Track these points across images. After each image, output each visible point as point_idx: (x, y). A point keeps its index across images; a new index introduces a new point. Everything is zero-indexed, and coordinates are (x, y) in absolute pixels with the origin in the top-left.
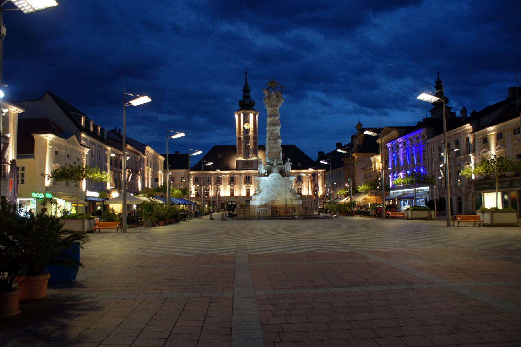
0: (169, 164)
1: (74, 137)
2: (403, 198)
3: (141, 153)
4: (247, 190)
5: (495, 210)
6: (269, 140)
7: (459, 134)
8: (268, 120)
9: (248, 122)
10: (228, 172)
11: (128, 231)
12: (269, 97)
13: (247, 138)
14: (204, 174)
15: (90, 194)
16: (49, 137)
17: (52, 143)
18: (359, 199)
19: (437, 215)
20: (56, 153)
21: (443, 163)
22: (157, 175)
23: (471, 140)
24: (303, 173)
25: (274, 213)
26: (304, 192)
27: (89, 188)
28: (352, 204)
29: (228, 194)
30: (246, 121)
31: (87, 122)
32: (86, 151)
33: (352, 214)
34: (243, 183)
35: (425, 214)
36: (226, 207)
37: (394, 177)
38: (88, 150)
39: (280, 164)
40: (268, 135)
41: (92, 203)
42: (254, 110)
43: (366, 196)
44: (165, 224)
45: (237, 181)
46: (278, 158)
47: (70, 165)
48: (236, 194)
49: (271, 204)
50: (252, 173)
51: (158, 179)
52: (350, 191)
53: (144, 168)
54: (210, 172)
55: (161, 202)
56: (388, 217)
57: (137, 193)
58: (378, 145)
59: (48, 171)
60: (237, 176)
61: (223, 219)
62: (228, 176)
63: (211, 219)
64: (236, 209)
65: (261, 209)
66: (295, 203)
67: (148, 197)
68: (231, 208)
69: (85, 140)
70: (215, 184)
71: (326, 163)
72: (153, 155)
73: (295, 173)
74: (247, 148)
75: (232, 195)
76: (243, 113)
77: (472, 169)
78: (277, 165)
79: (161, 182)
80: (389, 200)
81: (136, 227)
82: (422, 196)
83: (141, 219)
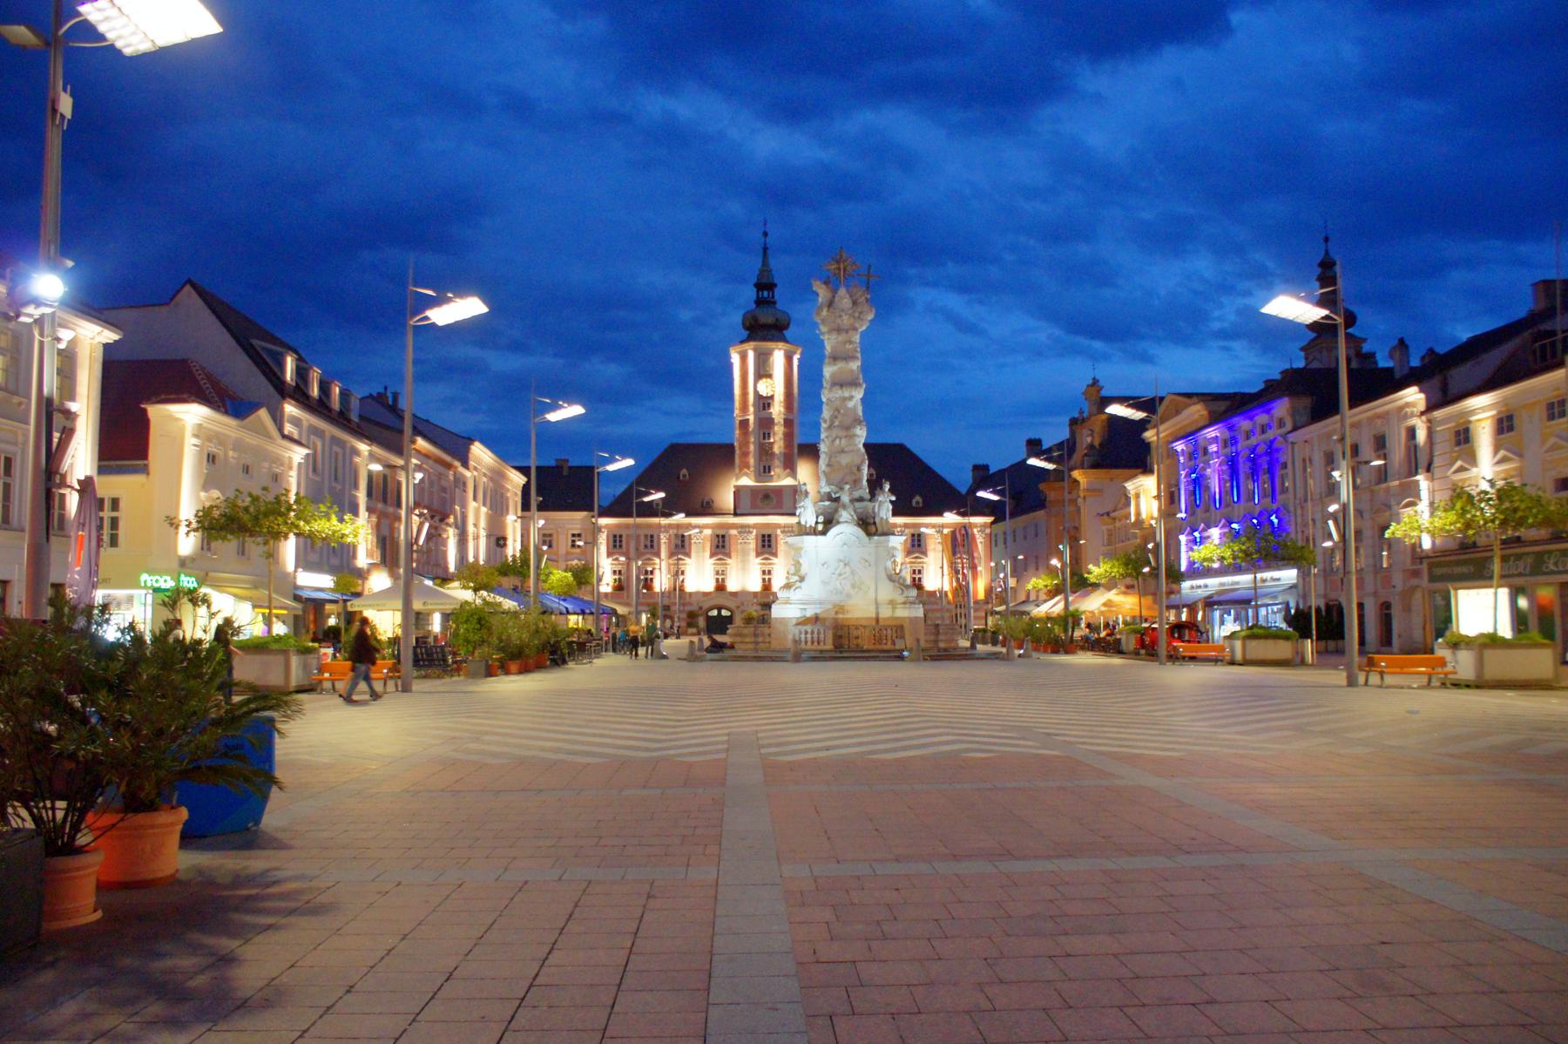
0: (538, 494)
1: (263, 413)
2: (1219, 603)
3: (457, 464)
5: (1491, 641)
6: (830, 427)
7: (1384, 416)
8: (828, 371)
9: (770, 376)
11: (414, 688)
12: (830, 304)
13: (766, 423)
14: (638, 526)
17: (199, 432)
20: (212, 458)
21: (1337, 499)
22: (503, 526)
23: (1421, 435)
24: (927, 526)
25: (842, 641)
27: (304, 562)
28: (1070, 619)
29: (709, 586)
30: (763, 372)
31: (301, 373)
32: (298, 454)
33: (1068, 647)
34: (753, 554)
35: (1283, 649)
36: (702, 622)
37: (1195, 541)
38: (304, 451)
39: (861, 499)
40: (826, 413)
42: (786, 341)
43: (1112, 595)
44: (525, 670)
45: (736, 546)
46: (856, 483)
47: (250, 495)
48: (732, 586)
49: (832, 615)
50: (778, 526)
51: (505, 539)
52: (1064, 580)
53: (464, 506)
54: (656, 520)
55: (509, 604)
56: (1174, 657)
57: (445, 579)
58: (1146, 446)
59: (187, 511)
60: (734, 532)
61: (692, 657)
62: (708, 532)
64: (726, 628)
65: (804, 628)
66: (902, 613)
67: (476, 590)
68: (718, 625)
69: (296, 422)
70: (671, 555)
71: (996, 498)
72: (492, 470)
73: (906, 526)
74: (765, 452)
75: (721, 587)
76: (755, 350)
77: (1422, 521)
78: (853, 501)
79: (513, 548)
80: (1178, 608)
81: (439, 677)
82: (1275, 597)
83: (455, 654)
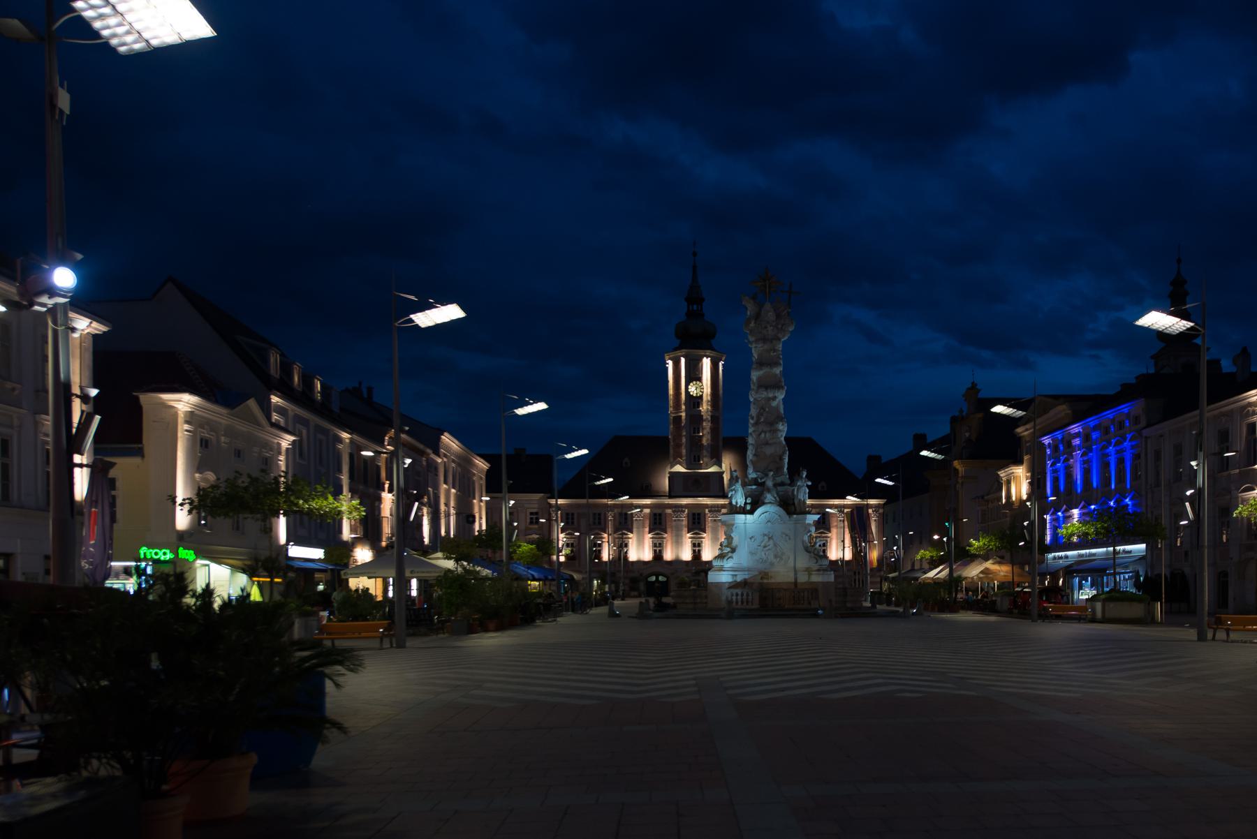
0: (509, 478)
1: (252, 403)
2: (1078, 571)
3: (429, 451)
4: (694, 545)
6: (756, 424)
7: (1229, 414)
8: (755, 375)
10: (648, 501)
11: (408, 644)
13: (695, 418)
14: (588, 505)
15: (296, 551)
16: (184, 402)
17: (191, 418)
18: (973, 571)
19: (1167, 612)
20: (205, 443)
21: (1192, 484)
22: (471, 506)
24: (831, 507)
26: (834, 553)
28: (953, 582)
29: (647, 555)
30: (694, 375)
32: (286, 441)
33: (953, 607)
34: (685, 529)
35: (1137, 610)
36: (642, 586)
37: (1057, 519)
38: (292, 438)
39: (782, 484)
40: (753, 411)
41: (305, 571)
42: (713, 349)
43: (989, 565)
44: (500, 628)
46: (778, 470)
47: (249, 476)
48: (668, 555)
49: (759, 580)
50: (706, 506)
51: (474, 517)
52: (949, 552)
53: (436, 488)
54: (605, 501)
55: (486, 572)
56: (1045, 616)
57: (426, 551)
58: (1019, 439)
59: (182, 491)
60: (669, 511)
61: (642, 615)
62: (647, 511)
63: (612, 614)
64: (673, 592)
65: (734, 591)
66: (816, 578)
67: (457, 560)
68: (663, 589)
69: (281, 411)
70: (616, 531)
71: (891, 483)
72: (459, 456)
74: (695, 443)
75: (658, 556)
78: (775, 485)
79: (481, 524)
80: (1043, 576)
81: (426, 635)
82: (1127, 567)
83: (440, 615)
